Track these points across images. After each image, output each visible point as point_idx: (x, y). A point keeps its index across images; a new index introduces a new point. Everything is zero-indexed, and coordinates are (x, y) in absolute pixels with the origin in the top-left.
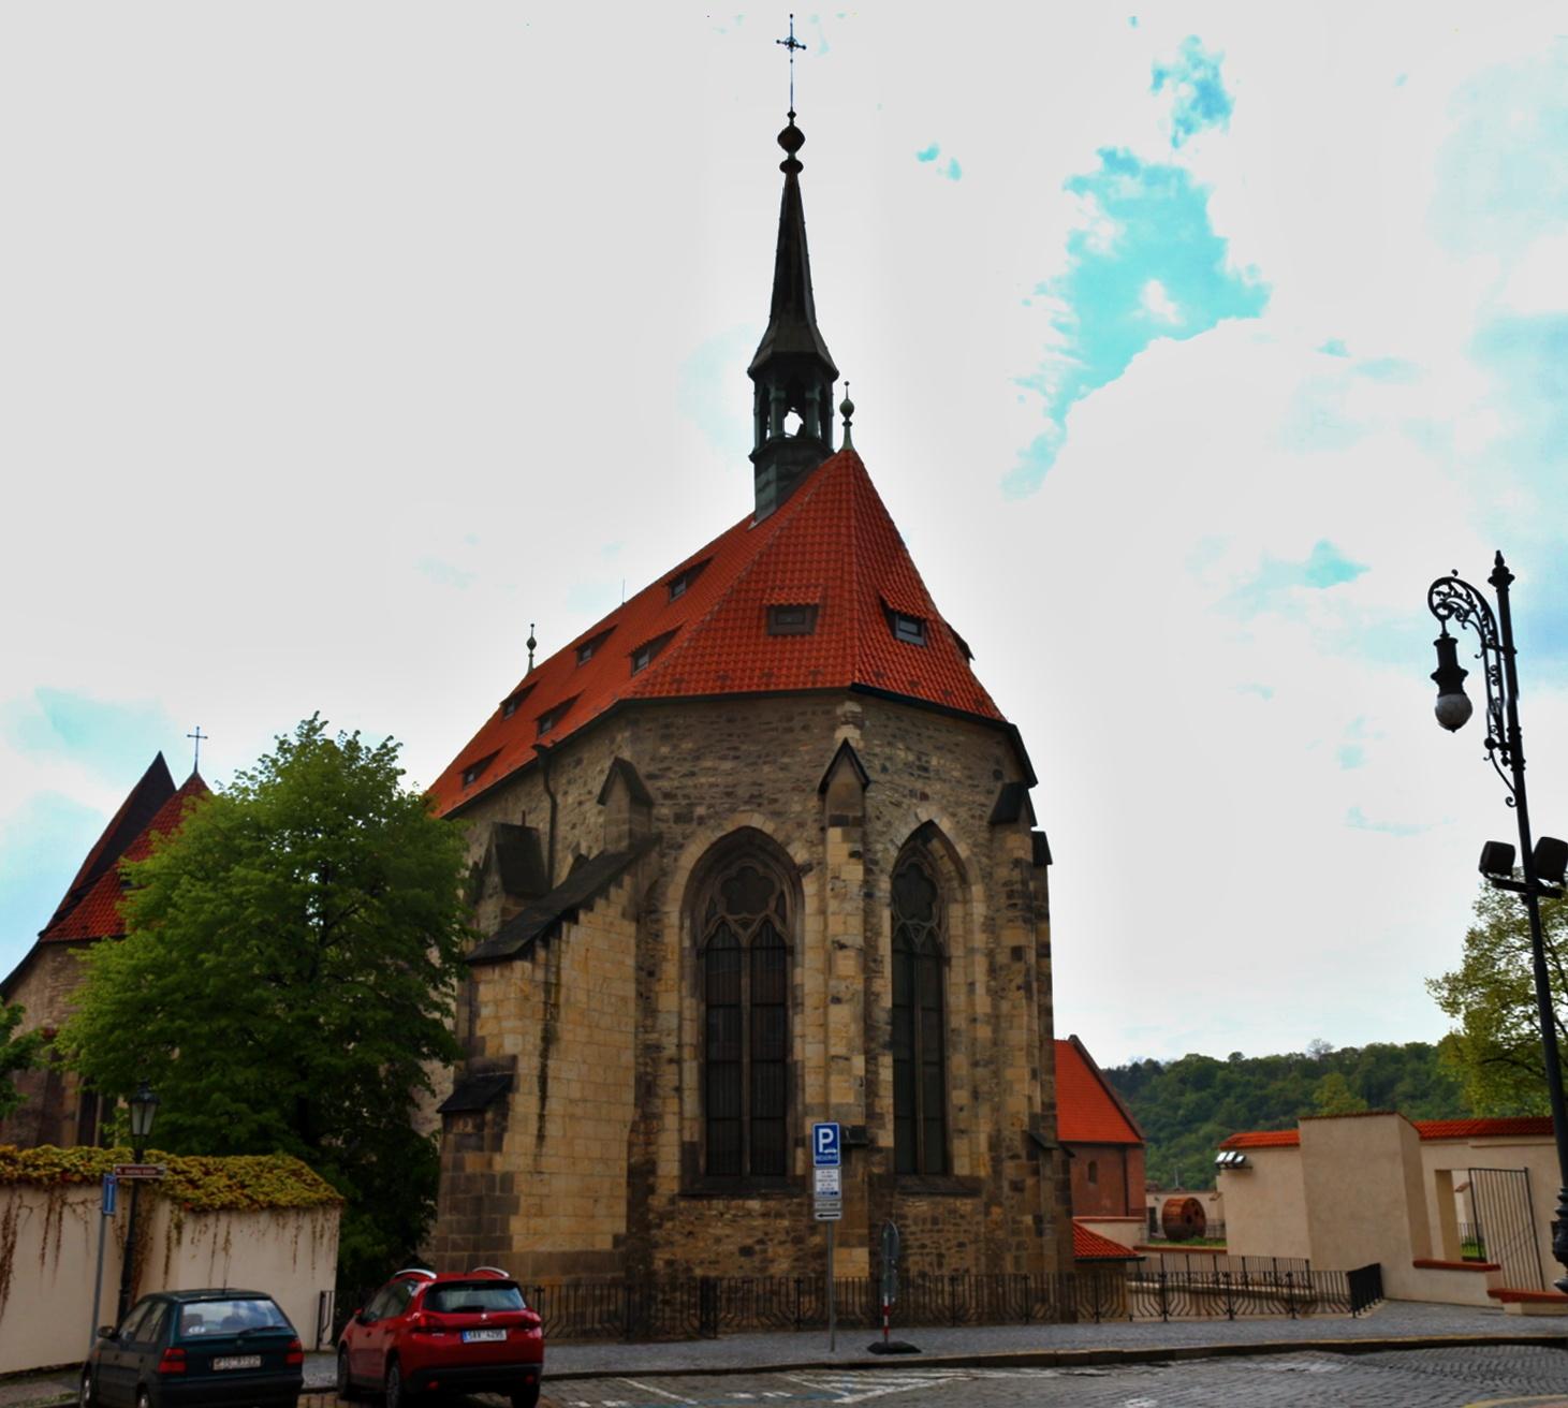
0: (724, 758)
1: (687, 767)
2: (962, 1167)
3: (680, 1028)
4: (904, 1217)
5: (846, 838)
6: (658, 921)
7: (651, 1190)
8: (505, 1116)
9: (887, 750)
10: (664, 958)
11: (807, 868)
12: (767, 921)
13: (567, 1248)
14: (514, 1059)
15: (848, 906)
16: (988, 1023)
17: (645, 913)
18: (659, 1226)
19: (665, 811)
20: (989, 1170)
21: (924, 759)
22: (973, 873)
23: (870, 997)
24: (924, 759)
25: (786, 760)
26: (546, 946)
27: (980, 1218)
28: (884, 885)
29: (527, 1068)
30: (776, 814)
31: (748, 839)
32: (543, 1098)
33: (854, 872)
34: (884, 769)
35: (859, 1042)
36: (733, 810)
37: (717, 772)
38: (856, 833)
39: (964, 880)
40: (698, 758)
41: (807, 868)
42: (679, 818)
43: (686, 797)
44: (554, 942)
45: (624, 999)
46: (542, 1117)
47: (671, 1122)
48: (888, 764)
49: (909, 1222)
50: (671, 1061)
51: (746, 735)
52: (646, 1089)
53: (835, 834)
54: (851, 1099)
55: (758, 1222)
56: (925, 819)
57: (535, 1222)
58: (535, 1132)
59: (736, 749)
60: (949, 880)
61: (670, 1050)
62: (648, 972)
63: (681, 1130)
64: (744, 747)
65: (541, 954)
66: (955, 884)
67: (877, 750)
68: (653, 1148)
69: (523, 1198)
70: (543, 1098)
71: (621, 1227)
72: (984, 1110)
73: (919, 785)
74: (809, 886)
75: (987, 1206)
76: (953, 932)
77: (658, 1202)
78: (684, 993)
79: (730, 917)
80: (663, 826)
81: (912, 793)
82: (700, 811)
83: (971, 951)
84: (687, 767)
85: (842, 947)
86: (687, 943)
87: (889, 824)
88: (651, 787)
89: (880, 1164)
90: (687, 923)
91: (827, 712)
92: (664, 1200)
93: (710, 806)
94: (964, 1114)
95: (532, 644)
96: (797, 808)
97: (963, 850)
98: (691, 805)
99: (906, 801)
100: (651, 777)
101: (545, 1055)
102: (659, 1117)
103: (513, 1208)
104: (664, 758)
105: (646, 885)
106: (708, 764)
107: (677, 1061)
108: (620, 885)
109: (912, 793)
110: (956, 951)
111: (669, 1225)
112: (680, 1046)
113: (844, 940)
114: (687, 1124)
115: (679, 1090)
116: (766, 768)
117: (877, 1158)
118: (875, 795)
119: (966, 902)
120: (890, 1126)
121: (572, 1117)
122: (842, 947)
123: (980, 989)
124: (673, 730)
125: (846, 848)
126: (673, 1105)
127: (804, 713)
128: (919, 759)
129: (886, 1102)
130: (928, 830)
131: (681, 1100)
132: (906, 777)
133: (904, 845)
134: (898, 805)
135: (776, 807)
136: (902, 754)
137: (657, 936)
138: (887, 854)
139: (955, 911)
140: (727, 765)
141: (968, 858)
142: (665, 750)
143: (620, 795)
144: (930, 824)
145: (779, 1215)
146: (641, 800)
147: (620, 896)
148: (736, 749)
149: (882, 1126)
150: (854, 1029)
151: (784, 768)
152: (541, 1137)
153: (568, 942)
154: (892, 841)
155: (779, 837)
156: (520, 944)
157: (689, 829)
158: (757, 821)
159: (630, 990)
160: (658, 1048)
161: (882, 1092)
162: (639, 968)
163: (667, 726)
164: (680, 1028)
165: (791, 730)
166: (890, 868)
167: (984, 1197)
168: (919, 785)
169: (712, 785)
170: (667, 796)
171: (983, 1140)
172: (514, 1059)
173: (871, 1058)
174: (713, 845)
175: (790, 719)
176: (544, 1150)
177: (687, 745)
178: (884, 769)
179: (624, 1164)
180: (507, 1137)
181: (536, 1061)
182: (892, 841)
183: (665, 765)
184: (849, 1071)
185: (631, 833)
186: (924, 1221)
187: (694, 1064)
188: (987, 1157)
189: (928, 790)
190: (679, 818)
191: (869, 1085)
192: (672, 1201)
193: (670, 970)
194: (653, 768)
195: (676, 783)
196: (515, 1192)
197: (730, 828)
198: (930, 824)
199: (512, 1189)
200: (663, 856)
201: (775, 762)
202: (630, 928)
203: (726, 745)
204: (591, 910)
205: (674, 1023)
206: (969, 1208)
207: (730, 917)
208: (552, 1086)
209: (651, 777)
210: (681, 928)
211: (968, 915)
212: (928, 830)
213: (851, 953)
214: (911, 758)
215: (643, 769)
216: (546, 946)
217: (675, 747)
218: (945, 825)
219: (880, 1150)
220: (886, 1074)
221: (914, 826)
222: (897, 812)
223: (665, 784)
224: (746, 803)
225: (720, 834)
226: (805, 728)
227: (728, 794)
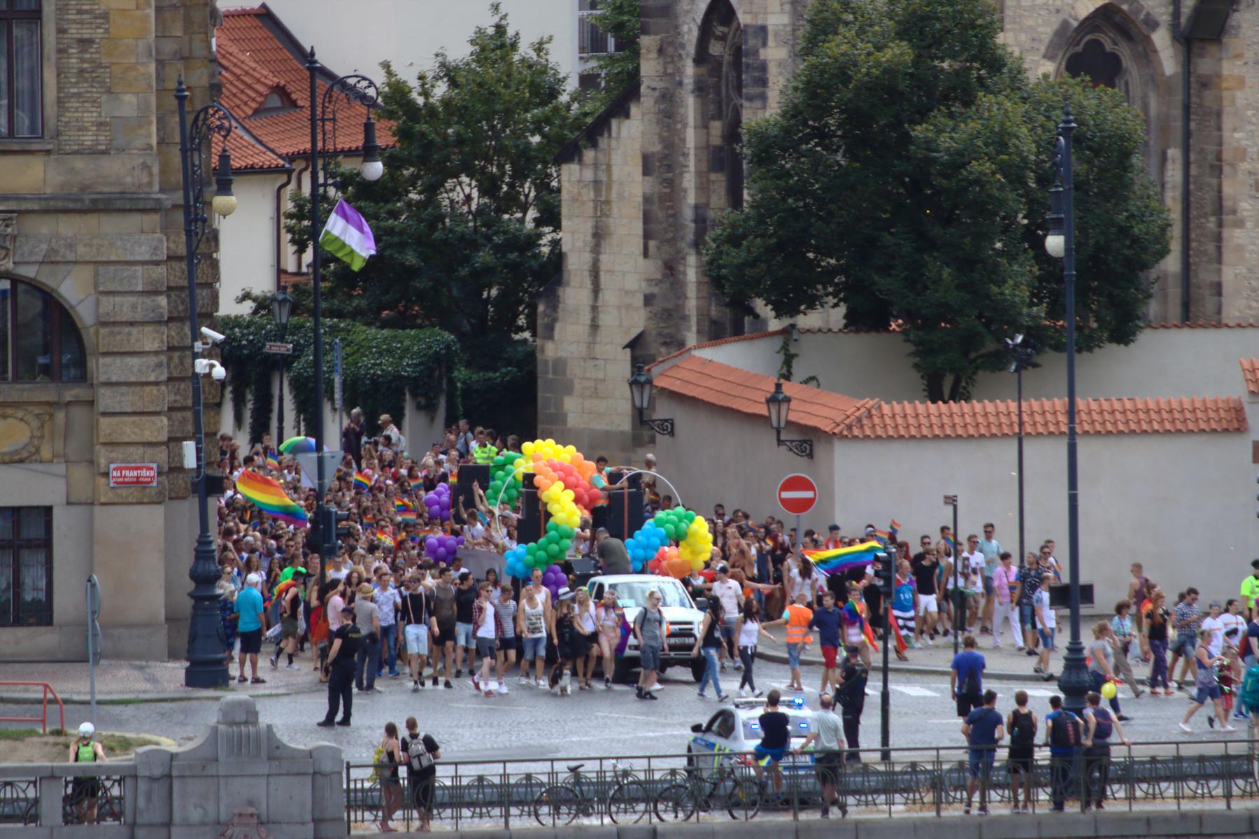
32: (596, 290)
44: (603, 142)
46: (594, 309)
57: (588, 404)
58: (589, 322)
69: (576, 382)
70: (596, 290)
101: (596, 249)
103: (568, 389)
149: (689, 329)
152: (594, 327)
153: (618, 138)
176: (598, 339)
181: (587, 257)
196: (569, 376)
199: (564, 373)
208: (603, 278)
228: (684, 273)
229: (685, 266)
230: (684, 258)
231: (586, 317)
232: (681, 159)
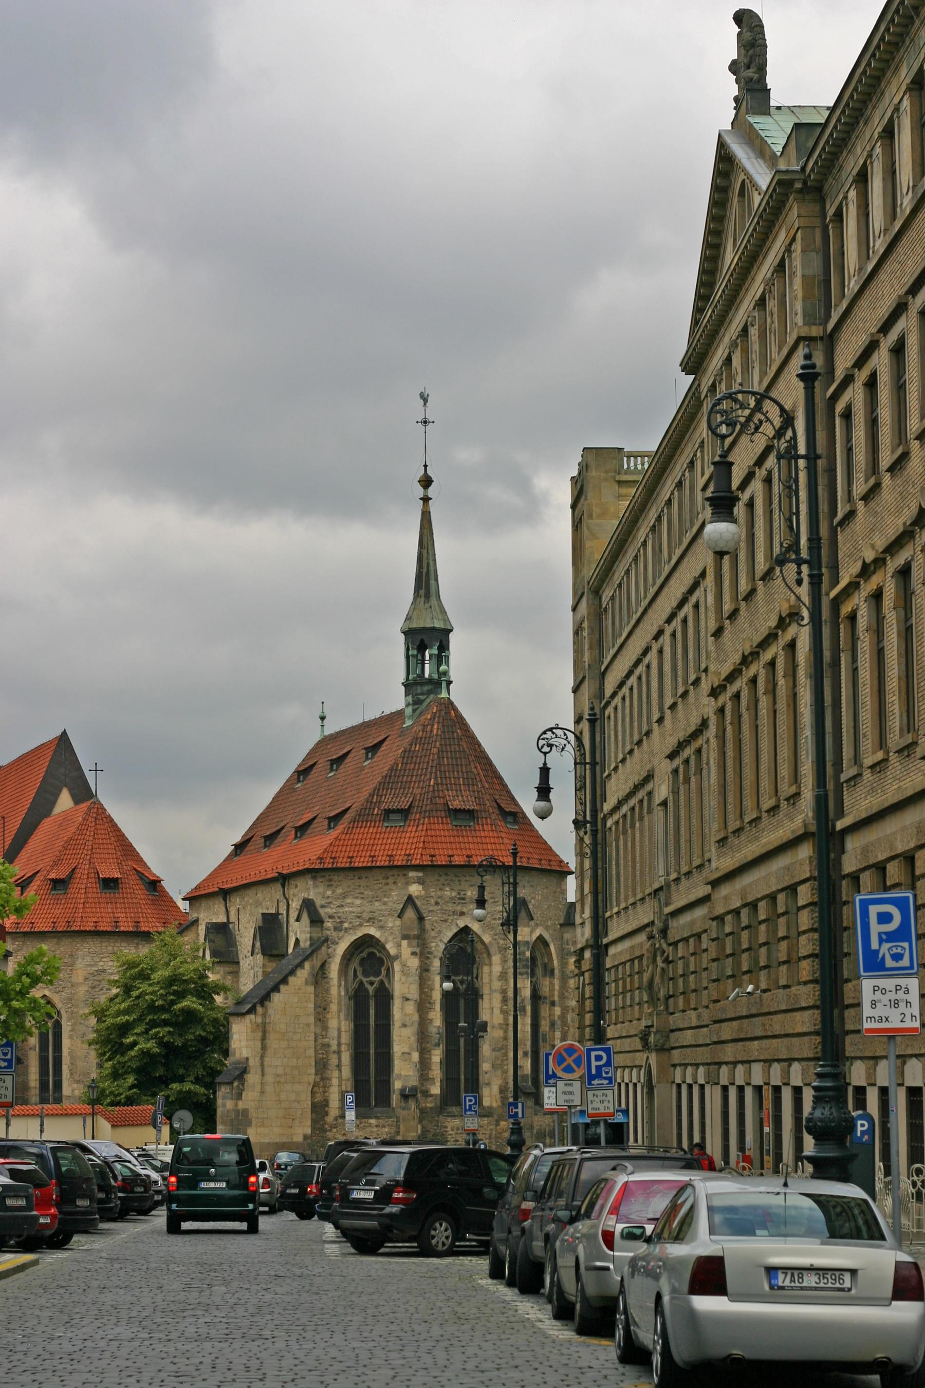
0: (357, 898)
1: (337, 903)
2: (486, 1102)
3: (339, 1036)
4: (446, 1127)
5: (409, 945)
6: (328, 983)
7: (327, 1114)
8: (243, 1085)
9: (439, 893)
10: (331, 1002)
11: (397, 957)
12: (382, 982)
13: (277, 1140)
14: (247, 1059)
15: (410, 979)
16: (501, 1028)
17: (319, 978)
18: (330, 1131)
19: (329, 925)
20: (500, 1104)
21: (462, 893)
22: (493, 949)
23: (423, 1023)
24: (462, 893)
25: (386, 899)
26: (262, 1005)
27: (493, 1127)
28: (436, 964)
29: (254, 1063)
30: (382, 927)
31: (366, 942)
33: (414, 963)
34: (437, 903)
35: (415, 1045)
36: (361, 925)
37: (354, 905)
38: (415, 942)
39: (489, 955)
40: (344, 898)
41: (397, 957)
42: (336, 929)
43: (339, 918)
45: (308, 1025)
47: (335, 1082)
48: (439, 900)
49: (449, 1129)
50: (334, 1052)
51: (367, 886)
52: (322, 1066)
53: (405, 943)
54: (411, 1073)
55: (375, 1129)
56: (462, 925)
57: (260, 1130)
59: (362, 893)
60: (482, 953)
61: (334, 1047)
62: (321, 1010)
63: (340, 1086)
64: (366, 893)
65: (259, 1009)
66: (485, 955)
67: (433, 894)
68: (327, 1094)
71: (308, 1131)
72: (499, 1073)
73: (459, 908)
74: (397, 967)
75: (497, 1124)
76: (484, 981)
77: (330, 1119)
78: (342, 1017)
79: (364, 980)
80: (329, 932)
81: (454, 913)
82: (346, 925)
83: (492, 991)
84: (337, 903)
85: (407, 999)
86: (343, 993)
87: (440, 932)
88: (322, 912)
89: (431, 1102)
90: (343, 983)
91: (405, 875)
92: (332, 1118)
93: (350, 923)
94: (487, 1076)
95: (323, 718)
96: (391, 925)
97: (486, 939)
98: (342, 922)
99: (451, 918)
100: (323, 906)
101: (262, 1057)
102: (330, 1079)
104: (328, 897)
105: (319, 964)
106: (350, 901)
107: (339, 1052)
108: (303, 968)
109: (454, 913)
110: (485, 991)
111: (335, 1130)
112: (339, 1045)
113: (408, 996)
114: (344, 1082)
115: (339, 1066)
116: (377, 904)
117: (430, 1099)
118: (429, 918)
119: (490, 965)
120: (438, 1084)
121: (279, 1082)
122: (407, 999)
123: (497, 1011)
124: (333, 883)
125: (409, 950)
126: (336, 1074)
127: (393, 875)
128: (459, 894)
129: (436, 1072)
130: (466, 930)
131: (340, 1070)
132: (451, 905)
133: (450, 941)
134: (445, 921)
135: (381, 923)
136: (448, 893)
137: (328, 991)
138: (438, 947)
139: (486, 969)
140: (358, 902)
141: (490, 942)
142: (329, 893)
143: (305, 917)
144: (466, 927)
145: (384, 1126)
146: (316, 921)
147: (303, 974)
148: (362, 893)
150: (413, 1039)
151: (385, 903)
152: (262, 1092)
154: (441, 940)
155: (382, 940)
156: (250, 1006)
157: (341, 934)
158: (372, 931)
159: (312, 1019)
160: (328, 1045)
161: (433, 1067)
162: (316, 1007)
163: (330, 880)
164: (339, 1036)
165: (387, 884)
166: (440, 955)
167: (496, 1117)
168: (459, 908)
169: (351, 912)
170: (331, 917)
171: (495, 1089)
172: (247, 1059)
173: (424, 1052)
174: (352, 943)
175: (388, 878)
177: (339, 891)
178: (437, 903)
179: (310, 1103)
180: (244, 1094)
182: (441, 940)
183: (329, 900)
184: (410, 1059)
185: (311, 938)
186: (458, 1129)
187: (348, 1053)
188: (498, 1097)
189: (465, 910)
190: (336, 929)
191: (424, 1065)
192: (336, 1119)
193: (334, 1007)
194: (323, 902)
195: (334, 911)
197: (359, 934)
198: (466, 927)
200: (329, 948)
201: (380, 901)
202: (311, 989)
203: (358, 891)
204: (279, 991)
205: (336, 1034)
206: (486, 1122)
207: (364, 980)
209: (323, 906)
210: (339, 986)
211: (491, 972)
212: (466, 930)
213: (412, 1003)
214: (454, 894)
215: (318, 902)
216: (262, 1005)
217: (333, 892)
218: (475, 927)
219: (432, 1096)
220: (436, 1056)
221: (455, 930)
222: (444, 925)
223: (328, 910)
224: (368, 921)
225: (356, 937)
226: (395, 883)
227: (359, 917)
228: (430, 1058)
229: (430, 1055)
230: (429, 1051)
231: (258, 1088)
232: (428, 1005)
